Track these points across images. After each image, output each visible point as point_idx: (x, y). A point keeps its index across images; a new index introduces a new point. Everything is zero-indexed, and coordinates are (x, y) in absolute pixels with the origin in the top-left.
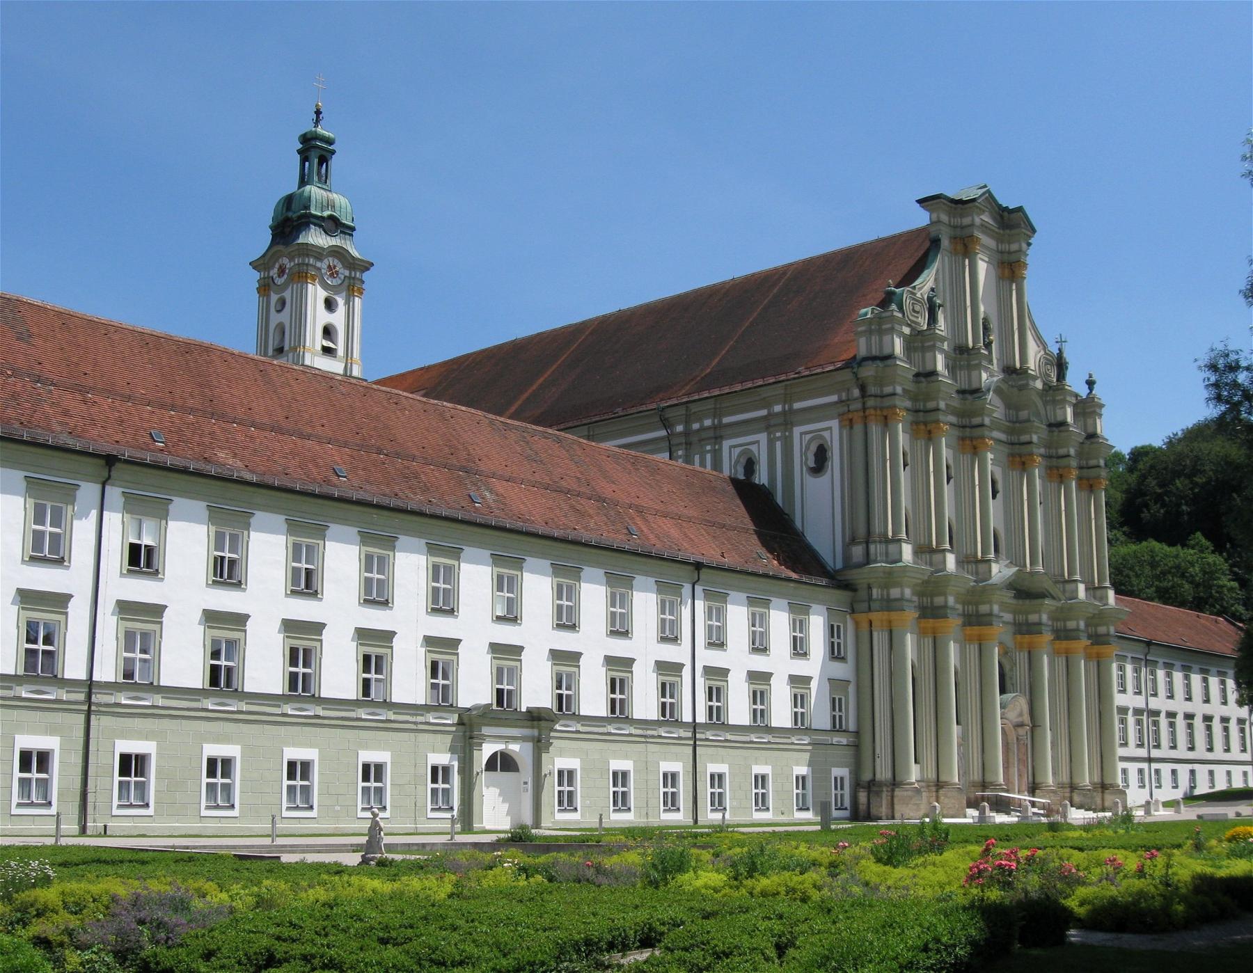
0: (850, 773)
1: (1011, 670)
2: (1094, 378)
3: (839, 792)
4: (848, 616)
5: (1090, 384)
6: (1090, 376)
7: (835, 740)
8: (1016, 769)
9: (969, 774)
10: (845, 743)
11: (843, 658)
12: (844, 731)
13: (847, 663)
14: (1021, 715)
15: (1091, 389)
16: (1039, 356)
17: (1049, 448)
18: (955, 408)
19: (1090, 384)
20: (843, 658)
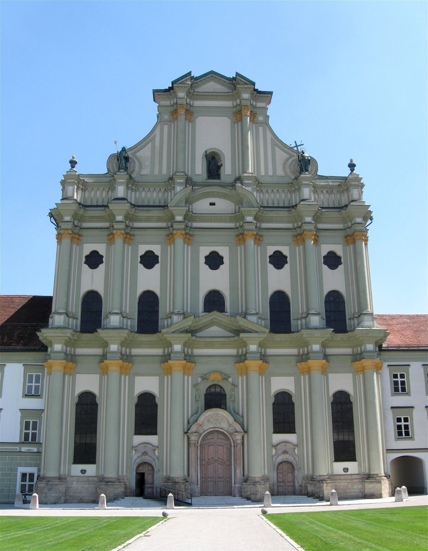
1: (233, 390)
2: (354, 162)
3: (27, 483)
5: (352, 166)
6: (351, 161)
7: (24, 449)
9: (163, 470)
10: (36, 451)
11: (39, 396)
13: (42, 398)
14: (230, 425)
15: (352, 170)
16: (290, 161)
17: (297, 222)
18: (159, 217)
19: (352, 166)
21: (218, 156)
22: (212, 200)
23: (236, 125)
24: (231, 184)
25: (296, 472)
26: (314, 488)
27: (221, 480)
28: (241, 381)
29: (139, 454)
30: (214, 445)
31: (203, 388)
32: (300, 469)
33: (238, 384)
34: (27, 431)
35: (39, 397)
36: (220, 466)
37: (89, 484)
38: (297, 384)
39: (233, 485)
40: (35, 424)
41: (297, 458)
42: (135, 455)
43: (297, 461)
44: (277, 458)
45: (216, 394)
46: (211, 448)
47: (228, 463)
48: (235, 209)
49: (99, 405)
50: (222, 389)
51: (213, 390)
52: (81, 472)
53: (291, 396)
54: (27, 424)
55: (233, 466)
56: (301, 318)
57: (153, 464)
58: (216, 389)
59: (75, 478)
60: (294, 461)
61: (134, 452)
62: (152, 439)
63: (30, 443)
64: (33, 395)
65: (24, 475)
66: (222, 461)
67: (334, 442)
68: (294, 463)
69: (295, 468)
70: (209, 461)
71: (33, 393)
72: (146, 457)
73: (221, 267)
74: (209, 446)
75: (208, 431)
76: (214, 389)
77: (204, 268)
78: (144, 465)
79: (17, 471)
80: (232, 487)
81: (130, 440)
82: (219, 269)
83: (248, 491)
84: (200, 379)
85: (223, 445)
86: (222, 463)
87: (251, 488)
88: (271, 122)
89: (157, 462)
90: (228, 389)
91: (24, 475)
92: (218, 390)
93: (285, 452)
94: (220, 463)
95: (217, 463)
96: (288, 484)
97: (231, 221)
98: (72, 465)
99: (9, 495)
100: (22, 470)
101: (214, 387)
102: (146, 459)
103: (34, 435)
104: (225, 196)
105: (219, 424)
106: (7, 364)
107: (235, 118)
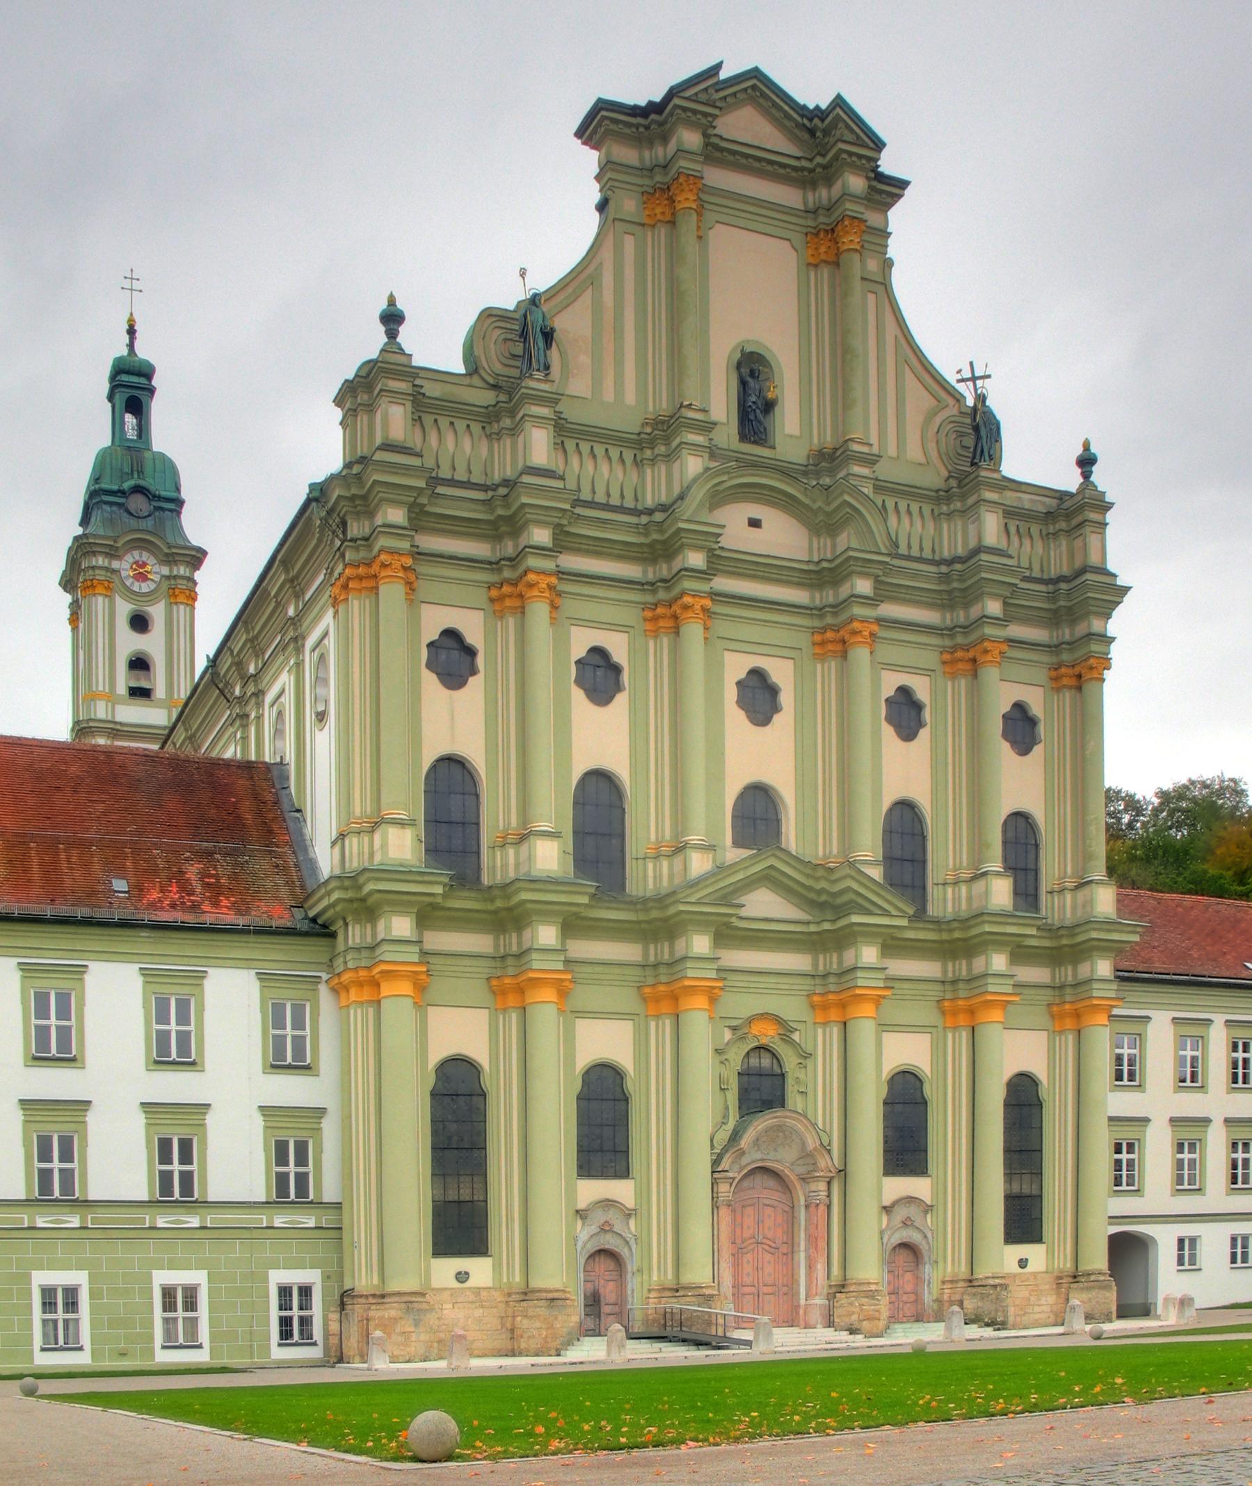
0: (326, 1277)
4: (323, 990)
8: (802, 1255)
9: (650, 1269)
10: (312, 1223)
12: (311, 1202)
20: (308, 1068)
21: (766, 370)
22: (756, 511)
23: (812, 274)
24: (803, 468)
25: (927, 1268)
26: (980, 1304)
27: (769, 1290)
28: (824, 1042)
29: (594, 1229)
30: (753, 1205)
31: (736, 1057)
32: (936, 1262)
33: (815, 1047)
34: (301, 1169)
35: (307, 1072)
36: (768, 1257)
37: (482, 1307)
38: (938, 1051)
39: (802, 1302)
40: (302, 1148)
41: (929, 1235)
42: (584, 1233)
43: (930, 1240)
44: (892, 1234)
45: (760, 1074)
46: (749, 1211)
47: (784, 1249)
48: (811, 548)
49: (491, 1100)
50: (775, 1061)
51: (754, 1061)
52: (457, 1278)
53: (921, 1082)
54: (281, 1148)
55: (802, 1256)
56: (956, 883)
57: (625, 1252)
58: (762, 1061)
59: (446, 1295)
60: (924, 1242)
61: (579, 1223)
62: (621, 1190)
63: (292, 1202)
64: (289, 1067)
65: (285, 1292)
66: (773, 1245)
67: (1005, 1197)
68: (924, 1247)
69: (926, 1259)
70: (746, 1244)
71: (289, 1060)
72: (609, 1237)
73: (776, 718)
74: (743, 1207)
75: (750, 1168)
76: (758, 1060)
77: (735, 718)
78: (597, 1259)
79: (267, 1281)
80: (798, 1306)
81: (571, 1193)
82: (770, 725)
83: (853, 1313)
84: (728, 1035)
85: (776, 1203)
86: (773, 1250)
87: (861, 1305)
88: (900, 282)
89: (634, 1247)
90: (790, 1061)
91: (285, 1292)
92: (766, 1061)
93: (907, 1223)
94: (767, 1248)
95: (760, 1250)
96: (905, 1298)
97: (799, 585)
98: (433, 1261)
99: (251, 1346)
100: (278, 1277)
101: (757, 1055)
102: (610, 1242)
103: (302, 1179)
104: (787, 503)
105: (775, 1150)
106: (210, 970)
107: (810, 252)
